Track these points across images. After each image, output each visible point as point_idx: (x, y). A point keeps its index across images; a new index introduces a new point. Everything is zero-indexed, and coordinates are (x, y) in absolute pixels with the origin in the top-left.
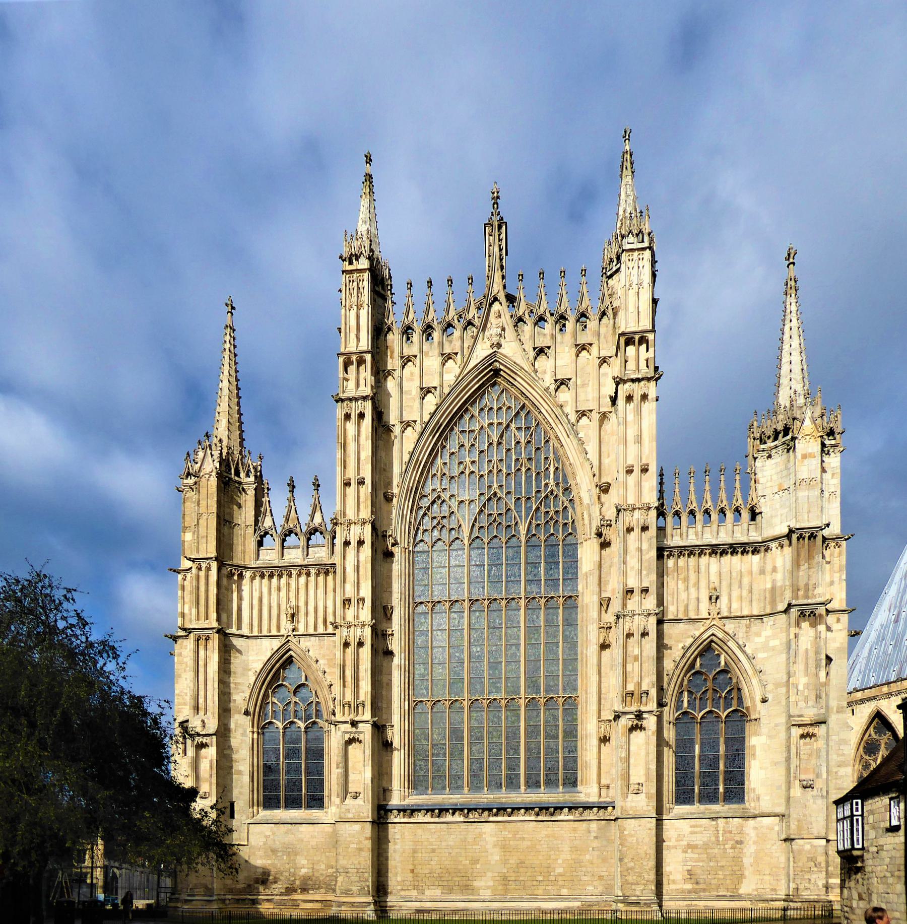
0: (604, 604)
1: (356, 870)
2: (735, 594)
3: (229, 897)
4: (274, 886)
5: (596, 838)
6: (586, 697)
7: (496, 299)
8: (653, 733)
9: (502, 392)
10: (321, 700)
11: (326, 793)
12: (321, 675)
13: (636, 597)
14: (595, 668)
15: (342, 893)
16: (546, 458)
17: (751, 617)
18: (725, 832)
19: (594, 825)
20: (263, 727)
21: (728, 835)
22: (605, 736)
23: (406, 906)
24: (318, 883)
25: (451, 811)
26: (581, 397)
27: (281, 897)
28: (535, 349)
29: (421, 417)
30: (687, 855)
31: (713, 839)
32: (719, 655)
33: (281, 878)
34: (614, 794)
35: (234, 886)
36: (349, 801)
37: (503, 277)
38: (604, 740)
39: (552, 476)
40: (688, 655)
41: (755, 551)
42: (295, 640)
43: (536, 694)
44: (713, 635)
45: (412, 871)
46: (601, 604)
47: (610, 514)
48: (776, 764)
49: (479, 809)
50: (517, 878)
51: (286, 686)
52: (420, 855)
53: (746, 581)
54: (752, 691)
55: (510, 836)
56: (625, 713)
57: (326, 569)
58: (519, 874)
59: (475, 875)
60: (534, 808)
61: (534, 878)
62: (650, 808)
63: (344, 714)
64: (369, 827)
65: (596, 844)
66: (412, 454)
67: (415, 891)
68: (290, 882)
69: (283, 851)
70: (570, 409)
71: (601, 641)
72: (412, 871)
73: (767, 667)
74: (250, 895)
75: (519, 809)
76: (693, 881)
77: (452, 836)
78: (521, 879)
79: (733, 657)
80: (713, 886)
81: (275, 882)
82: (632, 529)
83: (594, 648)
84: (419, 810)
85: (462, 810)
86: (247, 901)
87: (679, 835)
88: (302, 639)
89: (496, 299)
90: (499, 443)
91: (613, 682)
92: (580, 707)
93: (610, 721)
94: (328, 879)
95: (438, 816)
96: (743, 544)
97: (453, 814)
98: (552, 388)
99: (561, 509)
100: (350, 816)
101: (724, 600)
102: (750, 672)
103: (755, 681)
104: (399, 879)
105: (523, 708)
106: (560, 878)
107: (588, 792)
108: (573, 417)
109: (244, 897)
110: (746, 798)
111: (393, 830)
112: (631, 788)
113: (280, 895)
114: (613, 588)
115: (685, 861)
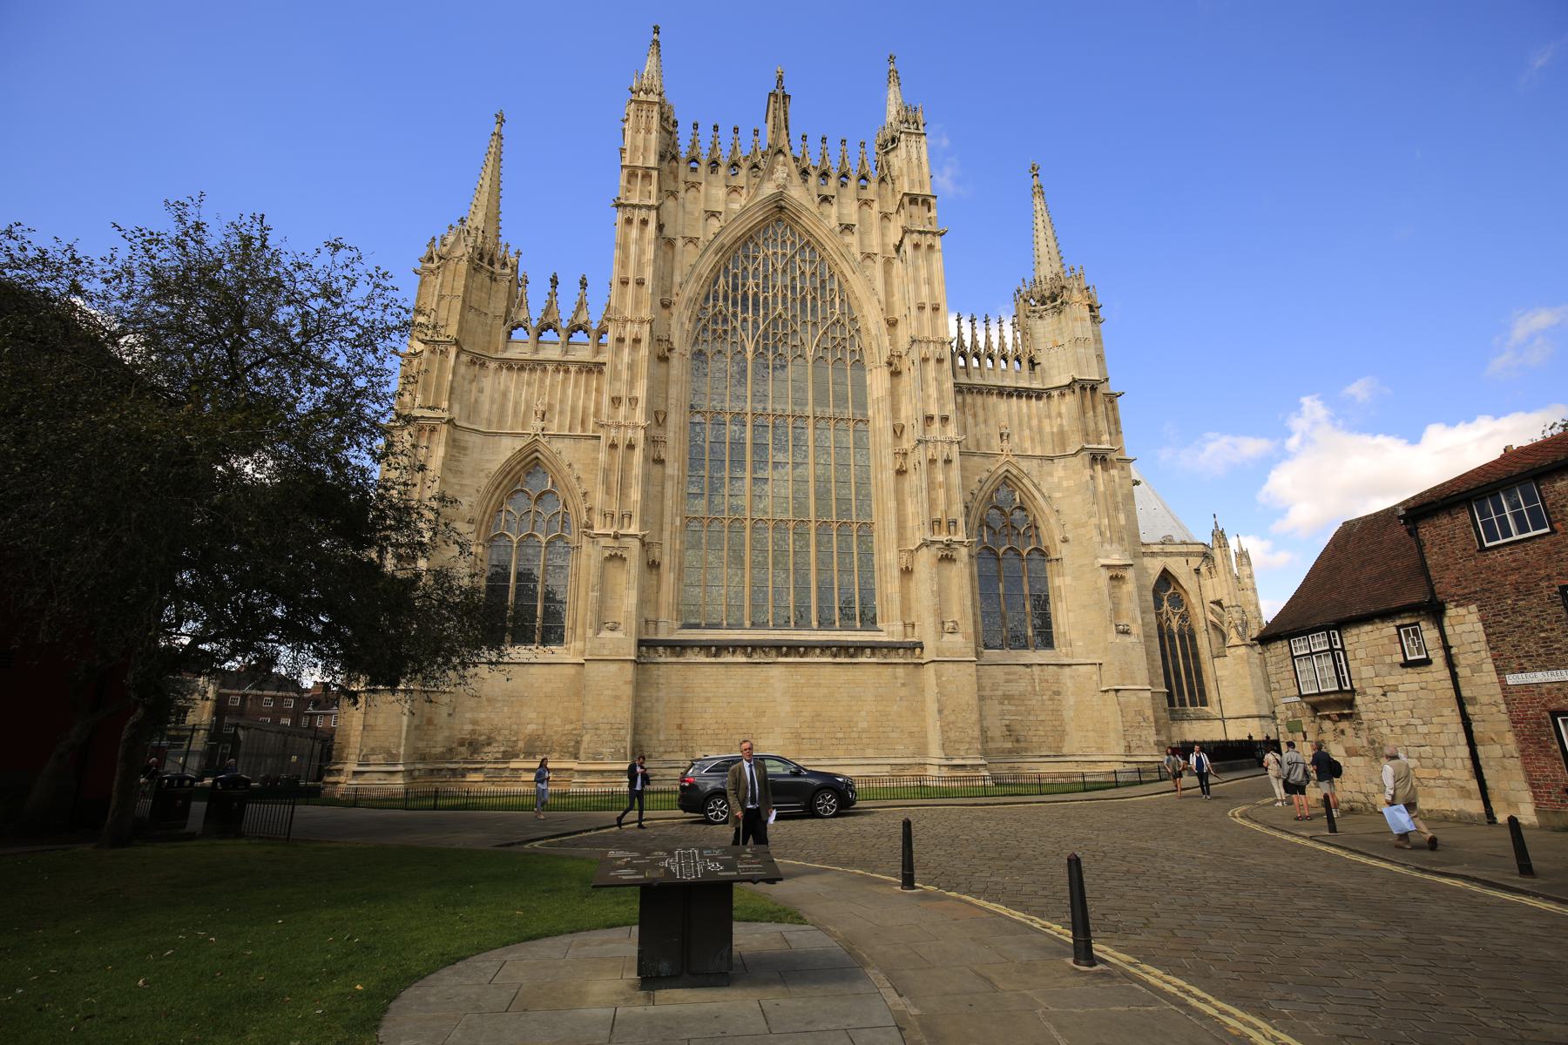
0: (898, 432)
1: (609, 726)
2: (1027, 433)
3: (420, 766)
4: (487, 749)
5: (903, 685)
6: (884, 525)
7: (780, 151)
8: (965, 565)
9: (786, 227)
10: (571, 510)
11: (568, 623)
12: (574, 481)
13: (937, 424)
14: (892, 496)
15: (588, 758)
16: (831, 290)
17: (1041, 458)
18: (1041, 681)
19: (900, 671)
20: (492, 540)
21: (1044, 684)
22: (907, 568)
23: (670, 775)
24: (550, 744)
25: (731, 649)
26: (866, 242)
27: (495, 766)
28: (819, 196)
29: (705, 235)
30: (1004, 707)
31: (1030, 688)
32: (1014, 491)
33: (498, 738)
34: (925, 632)
35: (428, 750)
36: (605, 634)
37: (788, 135)
38: (907, 572)
39: (837, 306)
40: (985, 488)
41: (1039, 397)
42: (543, 440)
43: (828, 517)
44: (1007, 471)
45: (680, 727)
46: (895, 431)
47: (903, 343)
48: (1084, 607)
49: (766, 647)
50: (812, 736)
51: (527, 492)
52: (690, 705)
53: (1035, 422)
54: (1051, 532)
55: (802, 681)
56: (934, 542)
57: (593, 368)
58: (814, 730)
59: (760, 731)
60: (831, 647)
61: (833, 736)
62: (969, 650)
63: (605, 526)
64: (630, 667)
65: (903, 692)
66: (693, 267)
67: (683, 753)
68: (510, 744)
69: (505, 701)
70: (855, 250)
71: (898, 467)
72: (680, 727)
73: (1063, 508)
74: (451, 763)
75: (814, 647)
76: (1012, 738)
77: (732, 681)
78: (817, 736)
79: (1029, 494)
80: (1035, 745)
81: (489, 744)
82: (928, 359)
83: (889, 475)
84: (692, 647)
85: (746, 647)
86: (444, 773)
87: (993, 684)
88: (554, 441)
89: (780, 151)
90: (784, 271)
91: (915, 510)
92: (875, 534)
93: (912, 551)
94: (564, 738)
95: (715, 656)
96: (1027, 389)
97: (734, 652)
98: (838, 229)
99: (848, 336)
100: (606, 652)
101: (1015, 438)
102: (1047, 510)
103: (1052, 521)
104: (662, 737)
105: (813, 532)
106: (864, 735)
107: (889, 631)
108: (859, 258)
109: (442, 766)
110: (1056, 644)
111: (656, 672)
112: (946, 626)
113: (495, 763)
114: (909, 412)
115: (1003, 713)
